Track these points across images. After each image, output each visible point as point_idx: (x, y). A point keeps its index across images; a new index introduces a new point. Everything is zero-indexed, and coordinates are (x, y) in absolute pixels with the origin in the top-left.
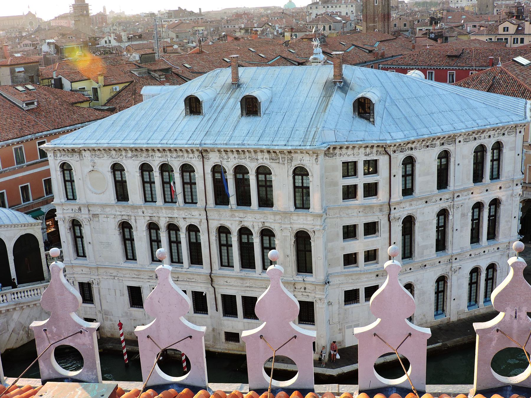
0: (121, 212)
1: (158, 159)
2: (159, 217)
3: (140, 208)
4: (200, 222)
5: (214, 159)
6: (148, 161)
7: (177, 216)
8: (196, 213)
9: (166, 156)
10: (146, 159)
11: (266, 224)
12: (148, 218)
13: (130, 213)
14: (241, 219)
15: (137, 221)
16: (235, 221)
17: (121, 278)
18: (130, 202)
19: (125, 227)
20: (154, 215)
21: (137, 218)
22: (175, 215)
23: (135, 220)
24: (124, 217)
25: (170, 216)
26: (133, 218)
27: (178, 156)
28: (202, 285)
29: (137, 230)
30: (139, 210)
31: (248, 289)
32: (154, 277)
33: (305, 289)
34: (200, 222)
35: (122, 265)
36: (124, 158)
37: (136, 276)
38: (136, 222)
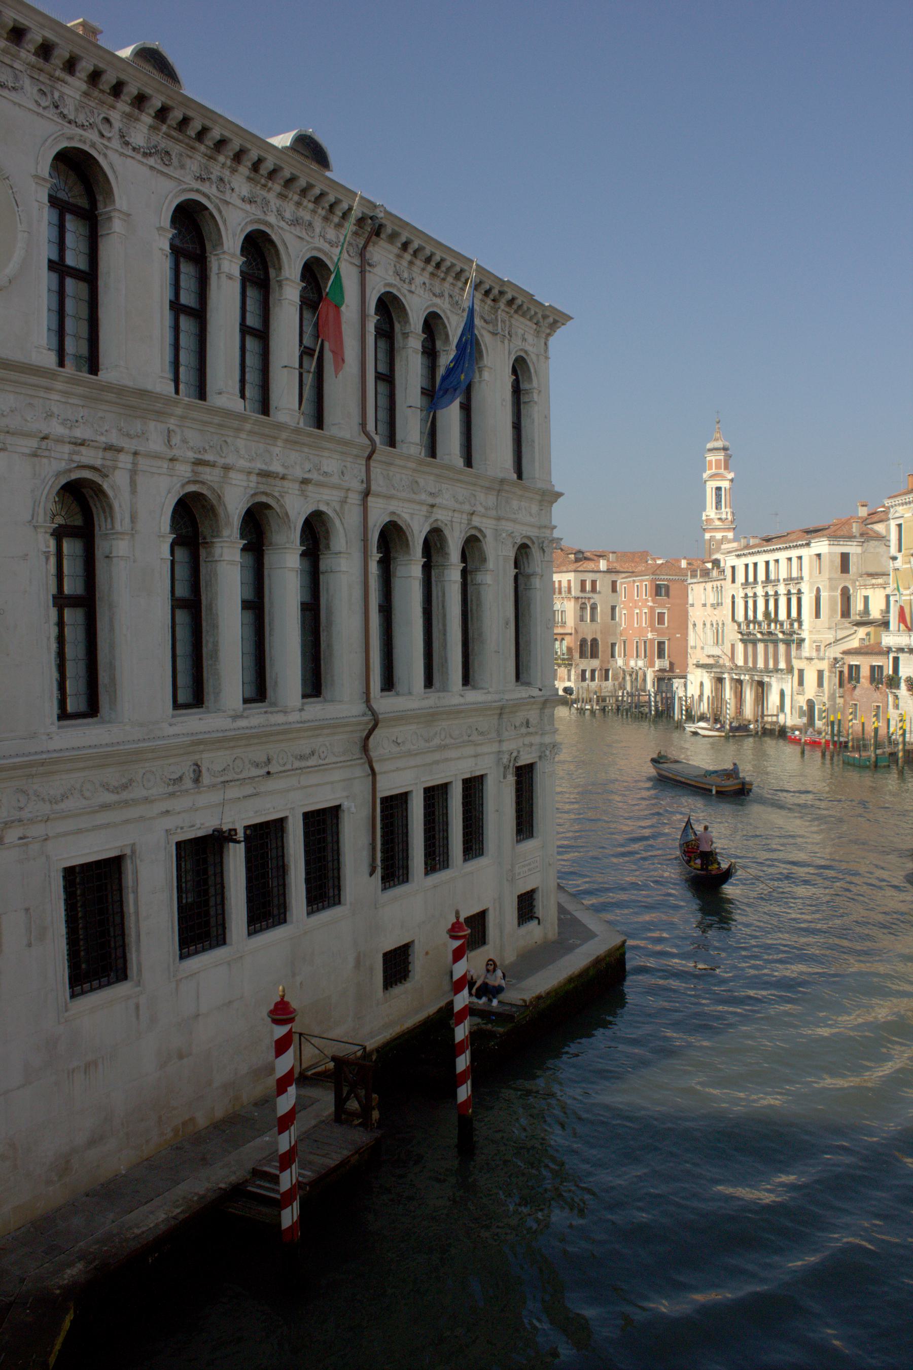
0: (66, 427)
1: (239, 203)
2: (227, 468)
3: (160, 415)
4: (344, 502)
5: (385, 271)
6: (207, 194)
7: (280, 470)
8: (331, 464)
9: (266, 202)
10: (196, 185)
11: (476, 521)
12: (184, 470)
13: (114, 438)
14: (431, 501)
15: (140, 479)
16: (421, 503)
17: (37, 830)
18: (103, 375)
19: (81, 509)
20: (208, 457)
21: (143, 463)
22: (276, 467)
23: (133, 473)
24: (88, 456)
25: (259, 465)
26: (125, 460)
27: (296, 222)
28: (337, 775)
29: (133, 533)
30: (152, 425)
31: (437, 756)
32: (188, 783)
33: (528, 722)
34: (344, 502)
35: (52, 745)
36: (116, 144)
37: (113, 798)
38: (133, 484)
